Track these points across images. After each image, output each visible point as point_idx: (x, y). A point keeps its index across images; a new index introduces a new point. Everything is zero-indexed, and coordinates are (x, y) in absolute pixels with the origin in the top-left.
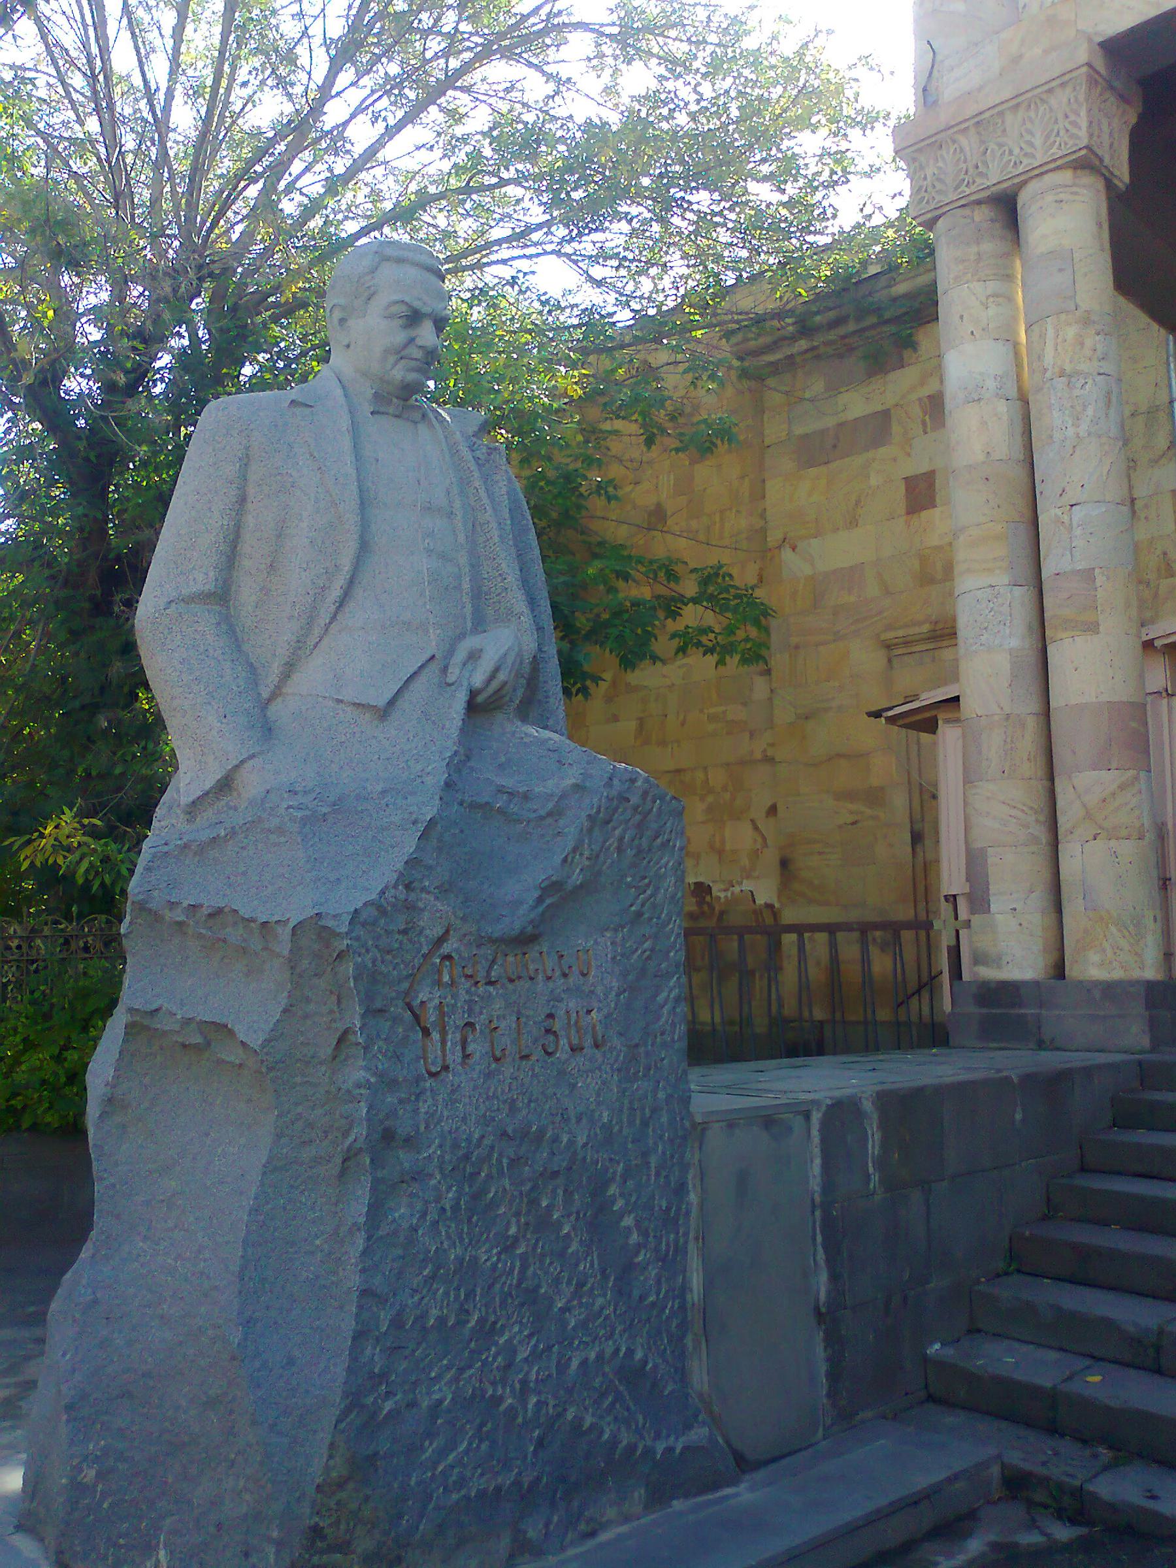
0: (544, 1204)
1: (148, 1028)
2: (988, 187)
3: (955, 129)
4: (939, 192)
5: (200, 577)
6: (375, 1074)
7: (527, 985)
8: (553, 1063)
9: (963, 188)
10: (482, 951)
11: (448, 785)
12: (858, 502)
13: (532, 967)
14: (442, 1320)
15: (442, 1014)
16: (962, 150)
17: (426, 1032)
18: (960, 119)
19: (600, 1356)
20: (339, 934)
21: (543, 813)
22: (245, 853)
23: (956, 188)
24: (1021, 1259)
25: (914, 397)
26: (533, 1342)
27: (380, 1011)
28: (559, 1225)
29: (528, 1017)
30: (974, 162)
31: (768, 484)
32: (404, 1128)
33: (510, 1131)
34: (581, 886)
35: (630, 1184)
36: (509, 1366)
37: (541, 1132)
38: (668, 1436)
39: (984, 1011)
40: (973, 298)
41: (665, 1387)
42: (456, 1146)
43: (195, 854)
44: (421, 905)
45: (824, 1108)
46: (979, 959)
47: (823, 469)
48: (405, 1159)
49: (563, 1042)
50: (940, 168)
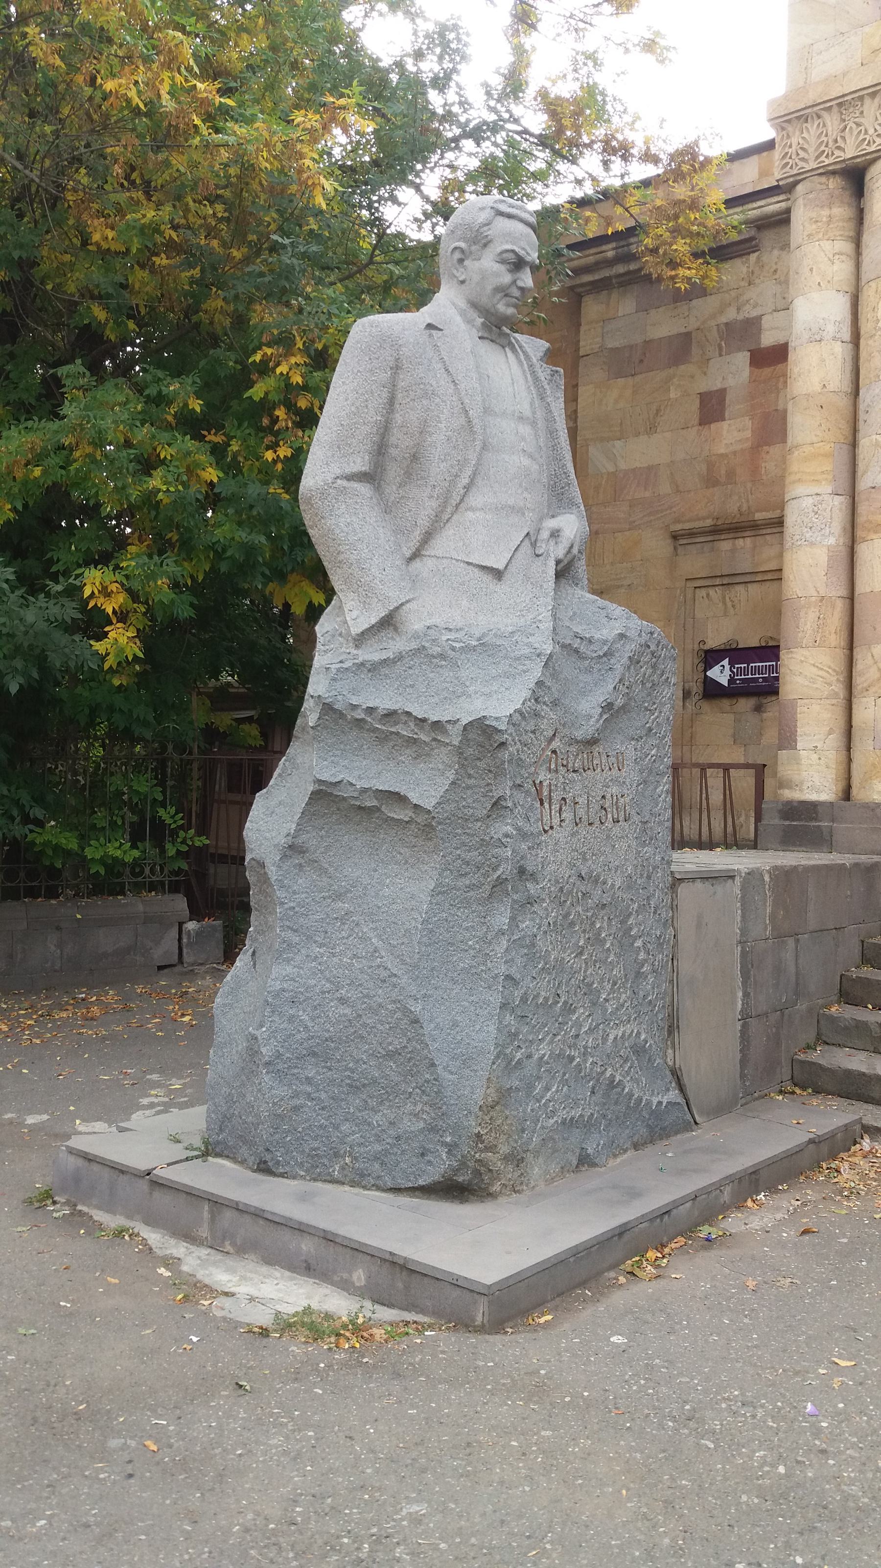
0: (598, 926)
1: (331, 794)
2: (844, 161)
3: (822, 106)
4: (803, 159)
5: (359, 460)
6: (516, 829)
9: (823, 158)
12: (658, 411)
15: (550, 791)
16: (824, 125)
17: (542, 804)
18: (826, 99)
20: (500, 731)
22: (411, 672)
23: (817, 157)
24: (850, 993)
25: (713, 323)
28: (604, 941)
30: (834, 137)
31: (581, 390)
36: (577, 1036)
37: (598, 876)
39: (787, 823)
40: (822, 254)
42: (557, 882)
43: (369, 671)
46: (782, 785)
47: (630, 380)
50: (803, 138)
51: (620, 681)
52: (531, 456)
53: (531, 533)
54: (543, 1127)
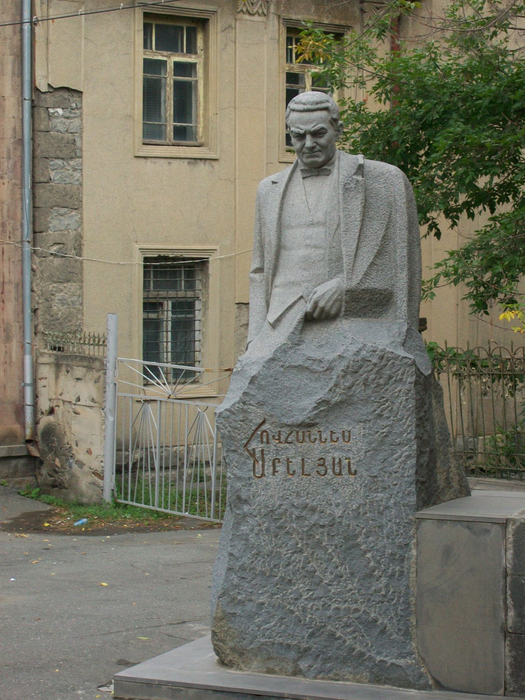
6: (232, 474)
7: (308, 445)
8: (322, 479)
10: (284, 429)
11: (272, 360)
13: (313, 437)
14: (263, 573)
19: (348, 610)
21: (325, 368)
26: (311, 593)
27: (235, 451)
29: (308, 459)
32: (244, 496)
33: (295, 504)
34: (341, 402)
35: (371, 539)
36: (296, 599)
38: (387, 656)
41: (391, 635)
44: (249, 410)
45: (518, 524)
48: (246, 508)
49: (330, 471)
51: (336, 385)
52: (316, 247)
53: (305, 296)
54: (259, 641)
